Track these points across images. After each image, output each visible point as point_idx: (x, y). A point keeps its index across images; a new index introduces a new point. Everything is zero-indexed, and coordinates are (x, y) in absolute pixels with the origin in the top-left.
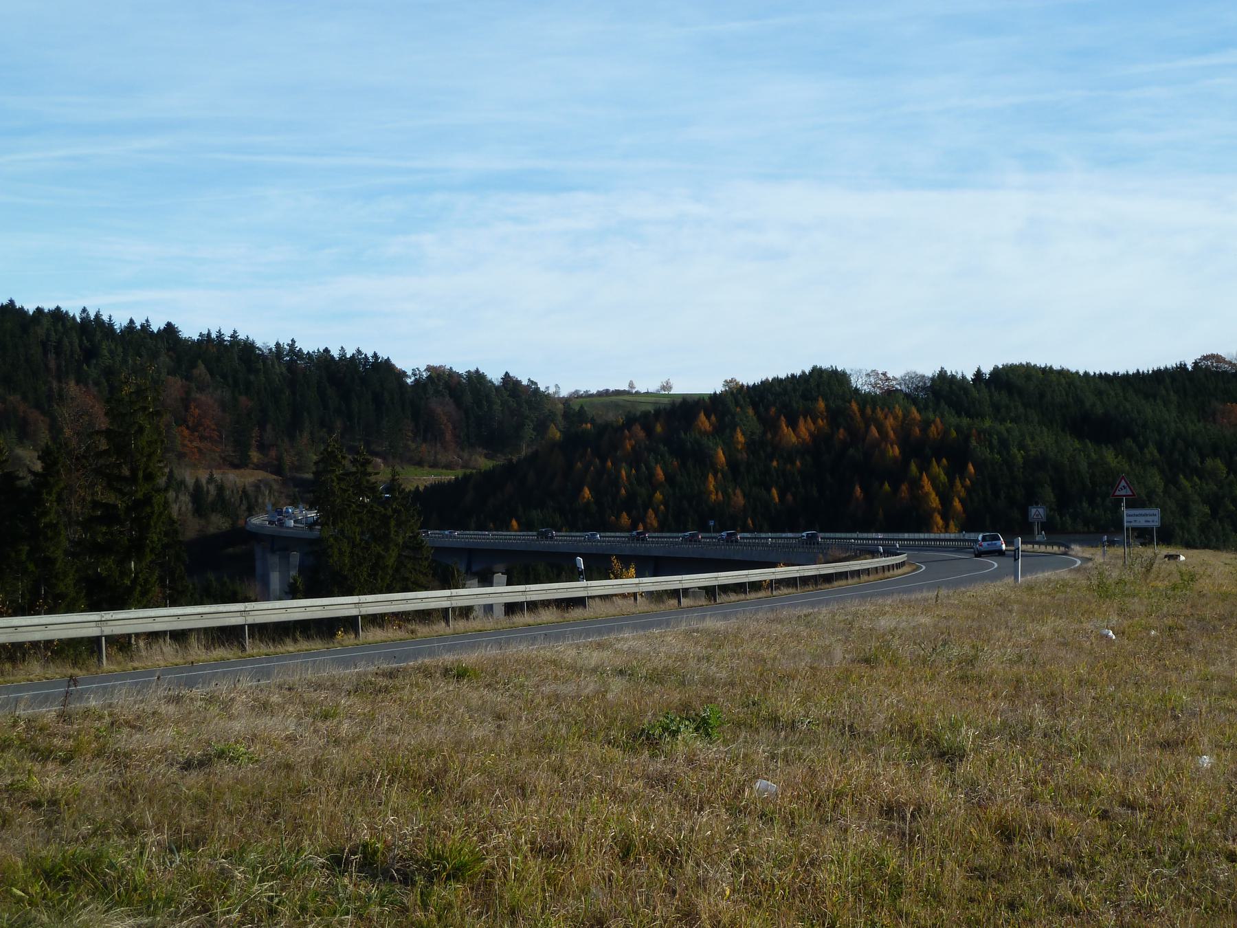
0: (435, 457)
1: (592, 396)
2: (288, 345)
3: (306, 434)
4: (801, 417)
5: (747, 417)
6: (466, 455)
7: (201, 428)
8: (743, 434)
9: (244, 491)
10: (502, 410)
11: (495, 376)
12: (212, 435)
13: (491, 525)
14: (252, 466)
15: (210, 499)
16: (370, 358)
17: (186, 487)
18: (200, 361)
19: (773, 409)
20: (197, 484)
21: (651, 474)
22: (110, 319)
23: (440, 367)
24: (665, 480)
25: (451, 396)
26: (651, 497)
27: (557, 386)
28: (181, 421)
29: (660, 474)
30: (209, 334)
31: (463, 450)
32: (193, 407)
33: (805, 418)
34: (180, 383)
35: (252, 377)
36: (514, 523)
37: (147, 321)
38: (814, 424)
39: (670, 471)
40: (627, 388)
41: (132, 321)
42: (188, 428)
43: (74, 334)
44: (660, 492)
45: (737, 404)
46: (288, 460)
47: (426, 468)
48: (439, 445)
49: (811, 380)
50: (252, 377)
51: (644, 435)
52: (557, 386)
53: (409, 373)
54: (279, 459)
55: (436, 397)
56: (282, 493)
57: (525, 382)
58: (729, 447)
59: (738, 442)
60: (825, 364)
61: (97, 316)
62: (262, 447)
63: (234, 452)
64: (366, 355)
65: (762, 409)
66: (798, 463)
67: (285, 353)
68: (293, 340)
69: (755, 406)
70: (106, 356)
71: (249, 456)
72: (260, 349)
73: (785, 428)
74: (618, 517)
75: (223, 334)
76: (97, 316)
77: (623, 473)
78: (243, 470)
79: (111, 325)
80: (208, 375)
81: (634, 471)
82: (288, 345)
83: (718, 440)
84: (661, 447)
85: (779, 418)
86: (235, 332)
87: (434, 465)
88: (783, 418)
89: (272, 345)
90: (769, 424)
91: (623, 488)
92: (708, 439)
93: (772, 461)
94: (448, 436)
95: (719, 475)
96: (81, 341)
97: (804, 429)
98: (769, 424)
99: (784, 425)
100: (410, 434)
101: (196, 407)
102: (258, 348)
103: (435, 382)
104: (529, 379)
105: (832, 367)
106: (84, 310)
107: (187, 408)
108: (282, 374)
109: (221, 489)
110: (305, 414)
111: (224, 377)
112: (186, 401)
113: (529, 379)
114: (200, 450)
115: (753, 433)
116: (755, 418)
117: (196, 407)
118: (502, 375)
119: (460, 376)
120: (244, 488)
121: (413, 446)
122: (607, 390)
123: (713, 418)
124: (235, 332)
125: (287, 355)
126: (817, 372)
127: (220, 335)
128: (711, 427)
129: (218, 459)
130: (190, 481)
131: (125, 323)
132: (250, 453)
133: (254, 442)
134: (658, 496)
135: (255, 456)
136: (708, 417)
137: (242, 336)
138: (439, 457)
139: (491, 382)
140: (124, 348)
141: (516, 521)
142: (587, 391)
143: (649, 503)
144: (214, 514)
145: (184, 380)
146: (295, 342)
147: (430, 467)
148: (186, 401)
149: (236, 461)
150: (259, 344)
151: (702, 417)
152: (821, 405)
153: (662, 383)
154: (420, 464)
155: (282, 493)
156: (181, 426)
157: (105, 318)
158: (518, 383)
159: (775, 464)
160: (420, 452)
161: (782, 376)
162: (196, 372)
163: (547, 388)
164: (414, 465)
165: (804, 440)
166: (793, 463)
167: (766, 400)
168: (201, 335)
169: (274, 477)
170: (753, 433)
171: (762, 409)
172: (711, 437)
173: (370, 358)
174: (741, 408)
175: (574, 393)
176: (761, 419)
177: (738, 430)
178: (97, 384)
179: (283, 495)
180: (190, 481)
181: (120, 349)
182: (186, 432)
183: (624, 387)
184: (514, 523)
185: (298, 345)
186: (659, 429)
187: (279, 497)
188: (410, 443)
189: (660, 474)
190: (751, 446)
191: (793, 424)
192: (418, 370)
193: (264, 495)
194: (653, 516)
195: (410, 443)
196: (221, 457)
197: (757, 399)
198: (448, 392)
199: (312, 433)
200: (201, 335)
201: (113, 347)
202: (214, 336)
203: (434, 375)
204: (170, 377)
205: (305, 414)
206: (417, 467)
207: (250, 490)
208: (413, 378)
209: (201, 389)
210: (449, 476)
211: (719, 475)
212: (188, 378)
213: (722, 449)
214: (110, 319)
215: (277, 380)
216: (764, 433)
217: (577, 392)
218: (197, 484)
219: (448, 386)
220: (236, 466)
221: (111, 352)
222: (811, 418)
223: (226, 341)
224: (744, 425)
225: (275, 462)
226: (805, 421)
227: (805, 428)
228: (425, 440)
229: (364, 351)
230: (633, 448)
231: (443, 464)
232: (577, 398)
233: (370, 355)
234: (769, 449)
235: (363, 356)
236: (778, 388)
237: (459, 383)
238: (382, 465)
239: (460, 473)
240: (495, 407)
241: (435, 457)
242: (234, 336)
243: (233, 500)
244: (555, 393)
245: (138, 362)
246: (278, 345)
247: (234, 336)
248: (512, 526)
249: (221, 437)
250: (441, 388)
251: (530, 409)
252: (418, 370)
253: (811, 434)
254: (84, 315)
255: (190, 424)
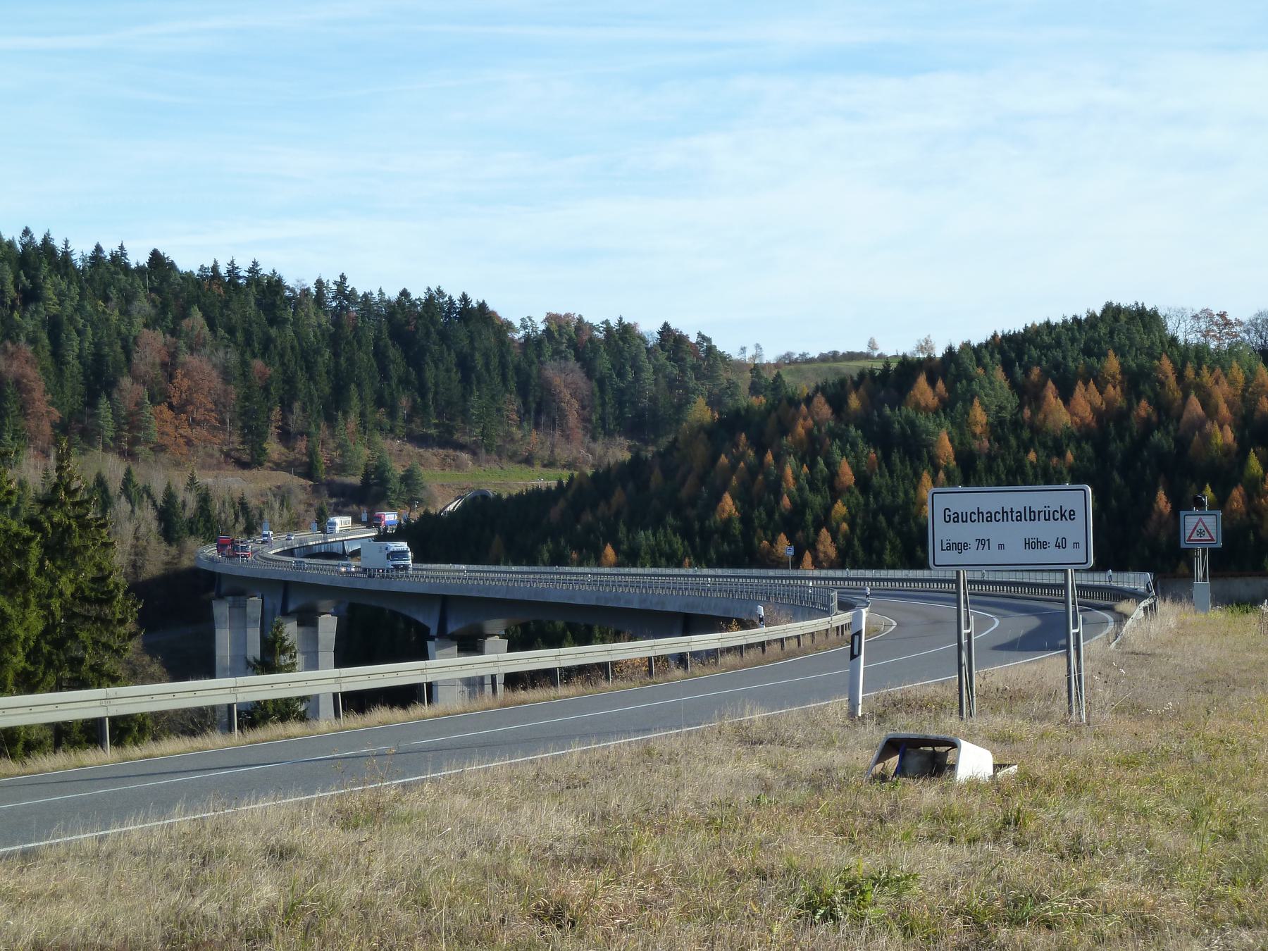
0: (552, 452)
1: (812, 361)
2: (335, 283)
3: (353, 419)
4: (1080, 383)
5: (991, 383)
6: (598, 447)
7: (190, 408)
8: (986, 409)
9: (244, 506)
10: (655, 379)
11: (649, 327)
12: (208, 418)
13: (574, 556)
14: (270, 465)
15: (188, 514)
16: (457, 302)
17: (150, 496)
18: (196, 307)
19: (1036, 371)
20: (170, 496)
21: (833, 475)
22: (66, 245)
23: (567, 315)
24: (855, 483)
25: (578, 359)
26: (828, 509)
27: (758, 346)
28: (156, 397)
29: (847, 475)
30: (215, 268)
31: (594, 439)
32: (179, 376)
33: (1086, 383)
34: (161, 339)
35: (273, 332)
36: (609, 551)
37: (122, 248)
38: (1101, 393)
39: (865, 468)
40: (865, 349)
41: (98, 249)
42: (171, 407)
43: (7, 267)
44: (843, 501)
45: (979, 362)
46: (323, 457)
47: (538, 468)
48: (558, 433)
49: (1100, 325)
50: (273, 332)
51: (830, 411)
52: (758, 346)
53: (517, 324)
54: (311, 453)
55: (555, 360)
56: (310, 505)
57: (693, 339)
58: (961, 426)
59: (976, 424)
60: (1126, 300)
61: (46, 240)
62: (286, 437)
63: (242, 443)
64: (450, 298)
65: (1018, 371)
66: (1070, 456)
67: (331, 295)
68: (342, 277)
69: (1008, 367)
70: (51, 299)
71: (265, 450)
72: (292, 290)
73: (1053, 400)
74: (773, 542)
75: (237, 268)
76: (46, 240)
77: (789, 471)
78: (255, 471)
79: (67, 254)
80: (207, 329)
81: (805, 469)
82: (335, 283)
83: (943, 420)
84: (852, 429)
85: (1044, 385)
86: (255, 264)
87: (550, 464)
88: (1050, 384)
89: (311, 285)
90: (1029, 394)
91: (785, 495)
92: (927, 417)
93: (1027, 452)
94: (573, 420)
95: (942, 475)
96: (17, 277)
97: (1082, 401)
98: (1029, 394)
99: (1051, 396)
100: (515, 417)
101: (185, 376)
102: (288, 288)
103: (554, 337)
104: (699, 334)
105: (1137, 304)
106: (26, 232)
107: (171, 377)
108: (320, 325)
109: (204, 499)
110: (353, 386)
111: (231, 331)
112: (169, 367)
113: (699, 334)
114: (189, 443)
115: (1001, 408)
116: (1006, 385)
117: (185, 376)
118: (658, 327)
119: (592, 327)
120: (243, 498)
121: (518, 434)
122: (835, 354)
123: (940, 385)
124: (255, 264)
125: (334, 298)
126: (1113, 312)
127: (233, 270)
128: (936, 398)
129: (217, 454)
130: (158, 490)
131: (89, 250)
132: (264, 446)
133: (273, 428)
134: (840, 508)
135: (274, 448)
136: (932, 382)
137: (265, 270)
138: (557, 451)
139: (642, 338)
140: (81, 288)
141: (613, 547)
142: (803, 355)
143: (824, 520)
144: (193, 538)
145: (168, 336)
146: (345, 279)
147: (544, 466)
148: (169, 367)
149: (246, 458)
150: (289, 281)
151: (922, 381)
152: (1112, 364)
153: (919, 341)
154: (528, 461)
155: (310, 505)
156: (159, 404)
157: (58, 244)
158: (680, 340)
159: (1032, 456)
160: (529, 443)
161: (1056, 319)
162: (185, 323)
163: (743, 349)
164: (520, 462)
165: (1082, 419)
166: (1061, 454)
167: (1026, 358)
168: (202, 268)
169: (303, 481)
170: (1001, 408)
171: (1018, 371)
172: (930, 414)
173: (457, 302)
174: (985, 368)
175: (784, 357)
176: (1014, 385)
177: (976, 402)
178: (33, 341)
179: (312, 509)
180: (158, 490)
181: (75, 290)
182: (168, 414)
183: (861, 347)
184: (609, 551)
185: (350, 284)
186: (854, 402)
187: (306, 511)
188: (514, 429)
189: (847, 475)
190: (998, 429)
191: (1066, 395)
192: (530, 320)
193: (272, 508)
194: (829, 539)
195: (514, 429)
196: (221, 451)
197: (1013, 355)
198: (572, 352)
199: (362, 415)
200: (202, 268)
201: (64, 285)
202: (223, 271)
203: (554, 328)
204: (145, 330)
205: (353, 386)
206: (523, 466)
207: (253, 503)
208: (522, 333)
209: (192, 349)
210: (541, 479)
211: (942, 475)
212: (174, 332)
213: (949, 433)
214: (66, 245)
215: (311, 335)
216: (1021, 407)
217: (789, 355)
218: (170, 496)
219: (572, 344)
220: (243, 465)
221: (61, 295)
222: (1096, 383)
223: (240, 277)
224: (986, 396)
225: (305, 459)
226: (1086, 390)
227: (1086, 400)
228: (537, 426)
229: (447, 291)
230: (809, 432)
231: (563, 463)
232: (789, 364)
233: (456, 297)
234: (1026, 434)
235: (447, 299)
236: (1046, 338)
237: (592, 340)
238: (470, 463)
239: (565, 475)
240: (644, 375)
241: (552, 452)
242: (254, 270)
243: (223, 516)
244: (754, 357)
245: (100, 309)
246: (319, 283)
247: (254, 270)
248: (606, 556)
249: (223, 422)
250: (563, 347)
251: (697, 379)
252: (530, 320)
253: (1095, 410)
254: (26, 240)
255: (175, 401)
